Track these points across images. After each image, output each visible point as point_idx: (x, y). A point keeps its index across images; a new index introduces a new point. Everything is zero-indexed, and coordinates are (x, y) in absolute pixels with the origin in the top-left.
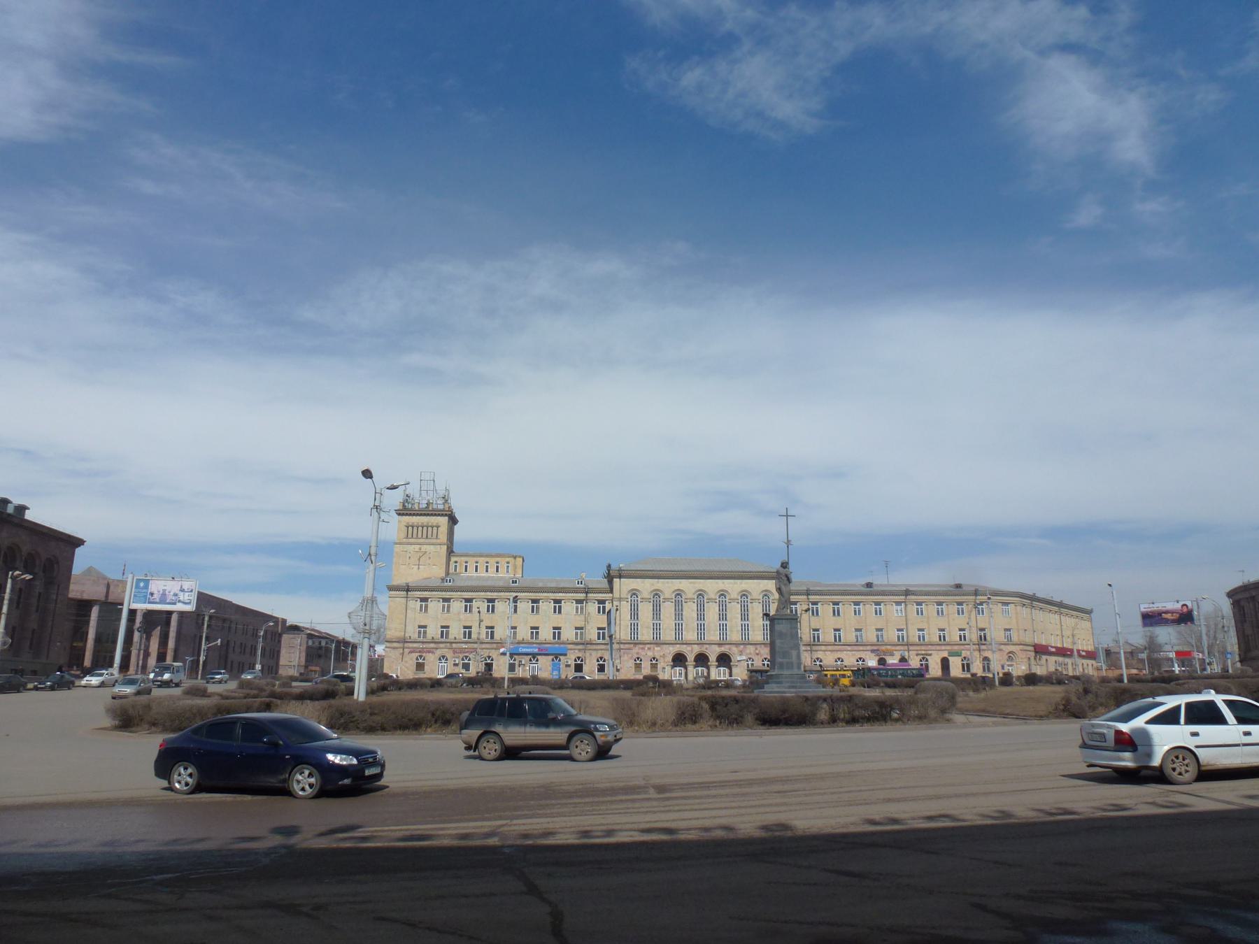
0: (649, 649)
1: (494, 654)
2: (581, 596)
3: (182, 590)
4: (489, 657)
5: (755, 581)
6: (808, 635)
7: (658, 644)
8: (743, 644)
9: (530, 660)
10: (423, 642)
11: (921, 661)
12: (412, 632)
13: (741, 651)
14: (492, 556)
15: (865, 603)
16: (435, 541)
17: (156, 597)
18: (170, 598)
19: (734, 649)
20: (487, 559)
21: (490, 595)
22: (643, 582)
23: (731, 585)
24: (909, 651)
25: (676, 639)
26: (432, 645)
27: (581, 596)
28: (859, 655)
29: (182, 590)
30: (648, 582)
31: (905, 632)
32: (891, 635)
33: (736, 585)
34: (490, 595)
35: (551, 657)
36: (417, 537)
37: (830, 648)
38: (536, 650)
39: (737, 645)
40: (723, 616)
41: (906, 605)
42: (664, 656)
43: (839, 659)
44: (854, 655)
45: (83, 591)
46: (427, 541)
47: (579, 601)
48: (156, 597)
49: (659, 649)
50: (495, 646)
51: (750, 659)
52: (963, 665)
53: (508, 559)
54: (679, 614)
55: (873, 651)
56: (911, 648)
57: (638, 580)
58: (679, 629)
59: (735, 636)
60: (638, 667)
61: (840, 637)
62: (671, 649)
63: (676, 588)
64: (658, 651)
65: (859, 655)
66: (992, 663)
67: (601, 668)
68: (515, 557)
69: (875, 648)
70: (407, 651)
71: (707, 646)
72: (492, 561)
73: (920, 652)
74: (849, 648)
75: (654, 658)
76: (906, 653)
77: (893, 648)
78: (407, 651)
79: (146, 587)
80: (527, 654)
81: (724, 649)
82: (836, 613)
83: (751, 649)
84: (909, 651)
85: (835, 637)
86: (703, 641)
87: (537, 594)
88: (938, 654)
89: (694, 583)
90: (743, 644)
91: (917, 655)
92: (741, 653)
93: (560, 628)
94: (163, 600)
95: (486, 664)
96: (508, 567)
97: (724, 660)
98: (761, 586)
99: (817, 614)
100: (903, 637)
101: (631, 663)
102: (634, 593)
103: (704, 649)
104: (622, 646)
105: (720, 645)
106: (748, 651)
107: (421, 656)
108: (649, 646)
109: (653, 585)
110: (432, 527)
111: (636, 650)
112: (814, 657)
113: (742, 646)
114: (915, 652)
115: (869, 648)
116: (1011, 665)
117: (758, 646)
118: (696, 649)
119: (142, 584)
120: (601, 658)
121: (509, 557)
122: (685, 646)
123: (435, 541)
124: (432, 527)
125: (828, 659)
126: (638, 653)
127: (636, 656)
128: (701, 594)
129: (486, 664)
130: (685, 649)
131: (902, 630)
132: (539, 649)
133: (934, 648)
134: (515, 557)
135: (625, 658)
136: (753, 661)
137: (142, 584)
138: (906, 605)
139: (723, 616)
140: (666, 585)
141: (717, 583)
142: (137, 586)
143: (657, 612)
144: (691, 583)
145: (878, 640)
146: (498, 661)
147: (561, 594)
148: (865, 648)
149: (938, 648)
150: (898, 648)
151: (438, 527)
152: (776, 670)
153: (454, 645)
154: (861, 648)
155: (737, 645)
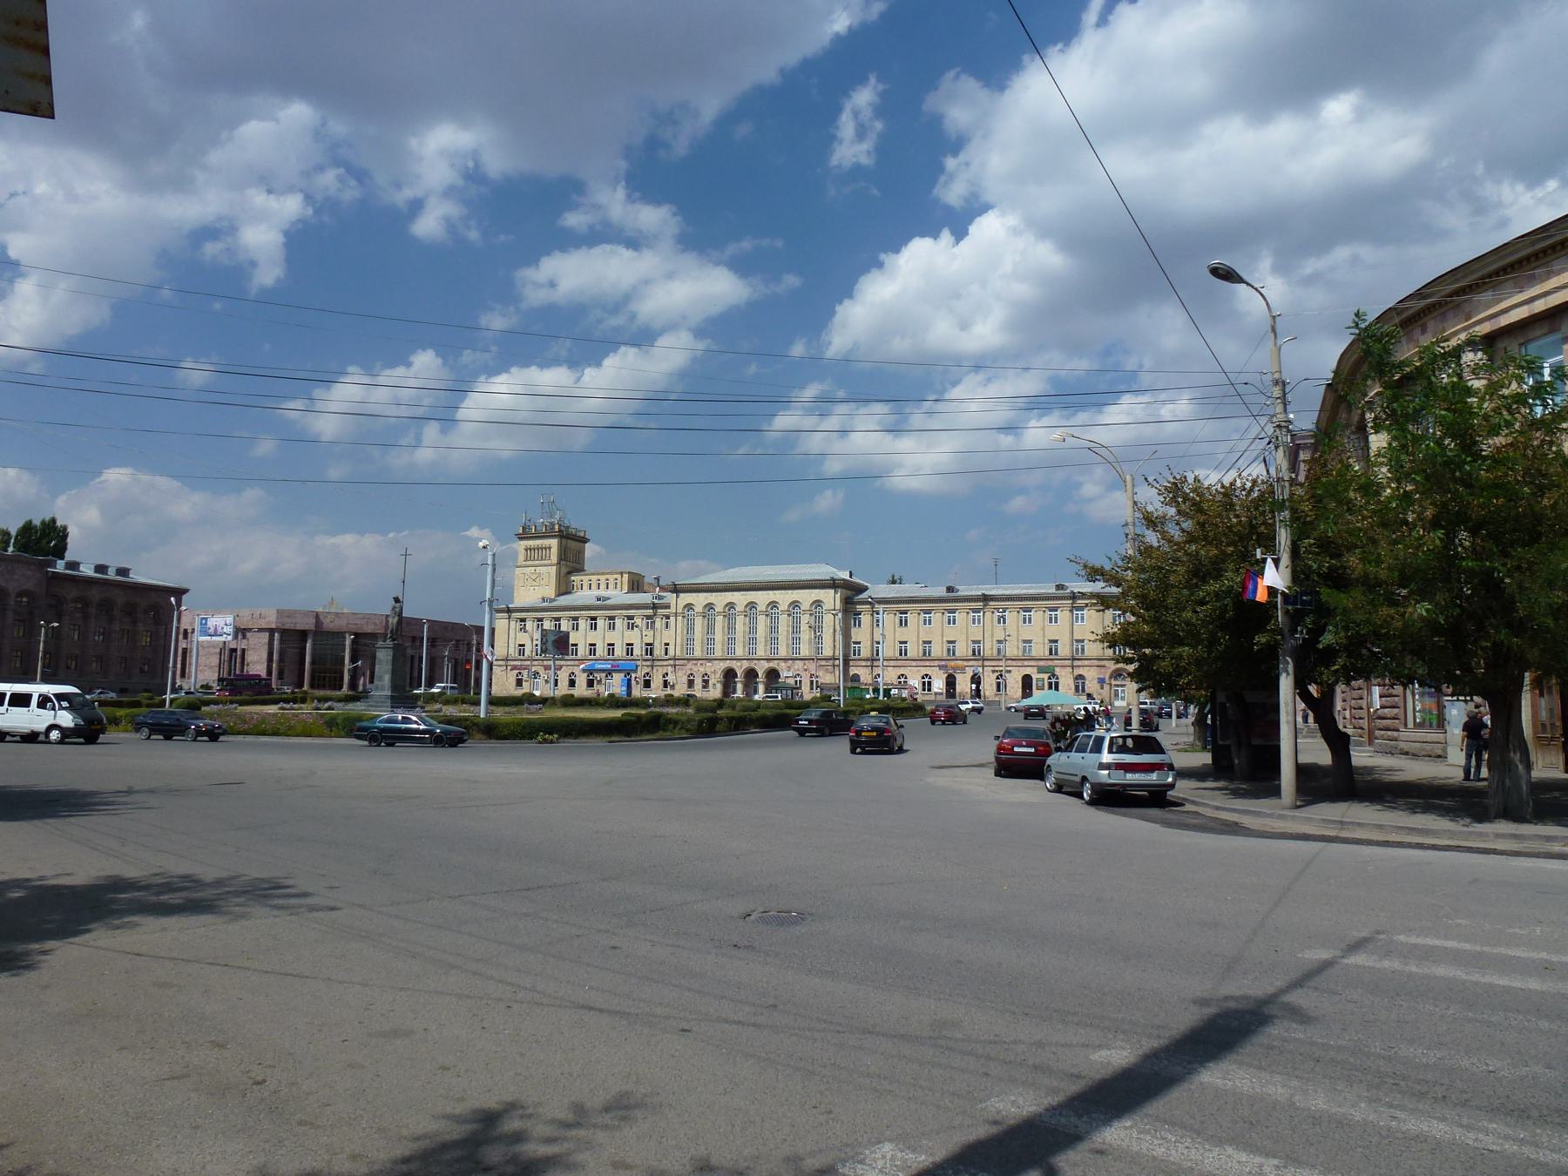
0: (702, 664)
1: (577, 671)
2: (650, 612)
3: (226, 625)
4: (573, 673)
5: (808, 591)
6: (869, 648)
7: (709, 660)
8: (791, 659)
9: (607, 676)
10: (543, 660)
11: (998, 678)
12: (513, 652)
13: (789, 667)
14: (603, 574)
15: (937, 610)
16: (546, 562)
17: (211, 631)
18: (219, 629)
19: (783, 664)
20: (608, 576)
21: (556, 614)
22: (698, 596)
23: (782, 596)
24: (983, 666)
25: (873, 654)
26: (528, 663)
27: (650, 612)
28: (924, 671)
29: (226, 625)
30: (702, 595)
31: (981, 645)
32: (962, 650)
33: (787, 596)
34: (556, 614)
35: (623, 675)
36: (538, 560)
37: (892, 663)
38: (609, 666)
39: (785, 660)
40: (773, 629)
41: (984, 612)
42: (715, 672)
43: (903, 675)
44: (919, 671)
45: (296, 623)
46: (543, 562)
47: (648, 617)
48: (211, 631)
49: (710, 664)
50: (577, 662)
51: (798, 675)
52: (924, 683)
53: (615, 576)
54: (731, 627)
55: (940, 667)
56: (986, 663)
57: (694, 594)
58: (731, 641)
59: (783, 652)
60: (691, 683)
61: (906, 650)
62: (722, 664)
63: (791, 601)
64: (711, 667)
65: (924, 671)
66: (1087, 682)
67: (666, 684)
68: (622, 573)
69: (943, 663)
70: (509, 668)
71: (756, 662)
72: (603, 578)
73: (997, 668)
74: (914, 663)
75: (706, 674)
76: (980, 669)
77: (965, 663)
78: (509, 668)
79: (206, 624)
80: (602, 671)
81: (773, 664)
82: (903, 623)
83: (800, 663)
84: (983, 666)
85: (901, 650)
86: (754, 656)
87: (612, 612)
88: (1019, 671)
89: (746, 595)
90: (791, 659)
91: (993, 671)
92: (789, 668)
93: (632, 645)
94: (215, 634)
95: (689, 680)
96: (616, 583)
97: (773, 674)
98: (813, 595)
99: (906, 625)
100: (979, 651)
101: (685, 679)
102: (731, 605)
103: (752, 665)
104: (677, 662)
105: (768, 660)
106: (796, 667)
107: (520, 673)
108: (701, 662)
109: (706, 598)
110: (546, 549)
111: (690, 665)
112: (874, 674)
113: (790, 662)
114: (992, 668)
115: (936, 663)
116: (1122, 686)
117: (807, 662)
118: (746, 664)
119: (204, 622)
120: (648, 674)
121: (617, 573)
122: (735, 662)
123: (546, 562)
124: (546, 549)
125: (889, 676)
126: (691, 669)
127: (689, 672)
128: (752, 605)
129: (689, 680)
130: (734, 665)
131: (979, 642)
132: (612, 666)
133: (1014, 663)
134: (622, 573)
135: (679, 674)
136: (817, 677)
137: (204, 622)
138: (984, 612)
139: (773, 629)
140: (720, 598)
141: (768, 594)
142: (201, 624)
143: (710, 628)
144: (743, 595)
145: (925, 654)
146: (580, 677)
147: (633, 611)
148: (932, 663)
149: (1019, 663)
150: (971, 663)
151: (550, 548)
152: (422, 688)
153: (545, 663)
154: (928, 663)
155: (785, 660)
